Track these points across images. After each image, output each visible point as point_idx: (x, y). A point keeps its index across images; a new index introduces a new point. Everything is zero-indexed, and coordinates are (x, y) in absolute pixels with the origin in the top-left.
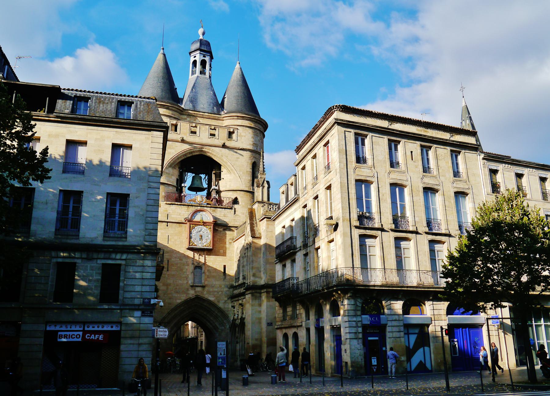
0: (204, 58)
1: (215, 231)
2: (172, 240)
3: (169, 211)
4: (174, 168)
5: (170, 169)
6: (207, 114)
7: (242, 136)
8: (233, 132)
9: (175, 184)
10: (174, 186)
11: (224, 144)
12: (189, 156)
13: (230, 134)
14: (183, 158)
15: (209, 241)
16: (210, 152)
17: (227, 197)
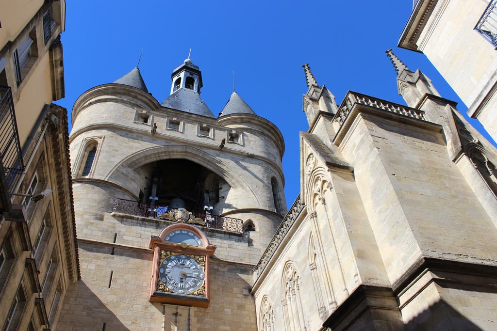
0: (191, 76)
1: (211, 272)
2: (121, 281)
3: (117, 230)
4: (136, 170)
5: (130, 170)
6: (195, 116)
7: (251, 141)
8: (237, 136)
9: (138, 196)
10: (134, 196)
11: (223, 141)
12: (165, 158)
13: (233, 138)
14: (154, 159)
15: (201, 284)
16: (201, 155)
17: (232, 224)
